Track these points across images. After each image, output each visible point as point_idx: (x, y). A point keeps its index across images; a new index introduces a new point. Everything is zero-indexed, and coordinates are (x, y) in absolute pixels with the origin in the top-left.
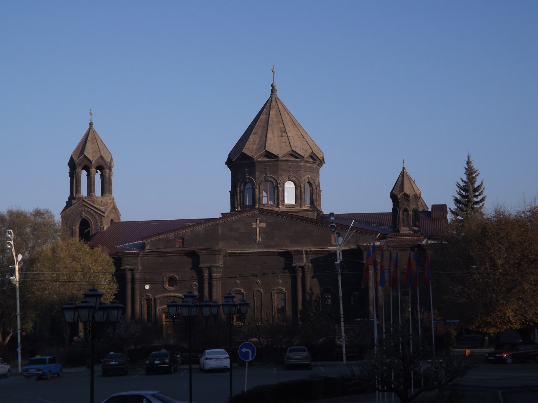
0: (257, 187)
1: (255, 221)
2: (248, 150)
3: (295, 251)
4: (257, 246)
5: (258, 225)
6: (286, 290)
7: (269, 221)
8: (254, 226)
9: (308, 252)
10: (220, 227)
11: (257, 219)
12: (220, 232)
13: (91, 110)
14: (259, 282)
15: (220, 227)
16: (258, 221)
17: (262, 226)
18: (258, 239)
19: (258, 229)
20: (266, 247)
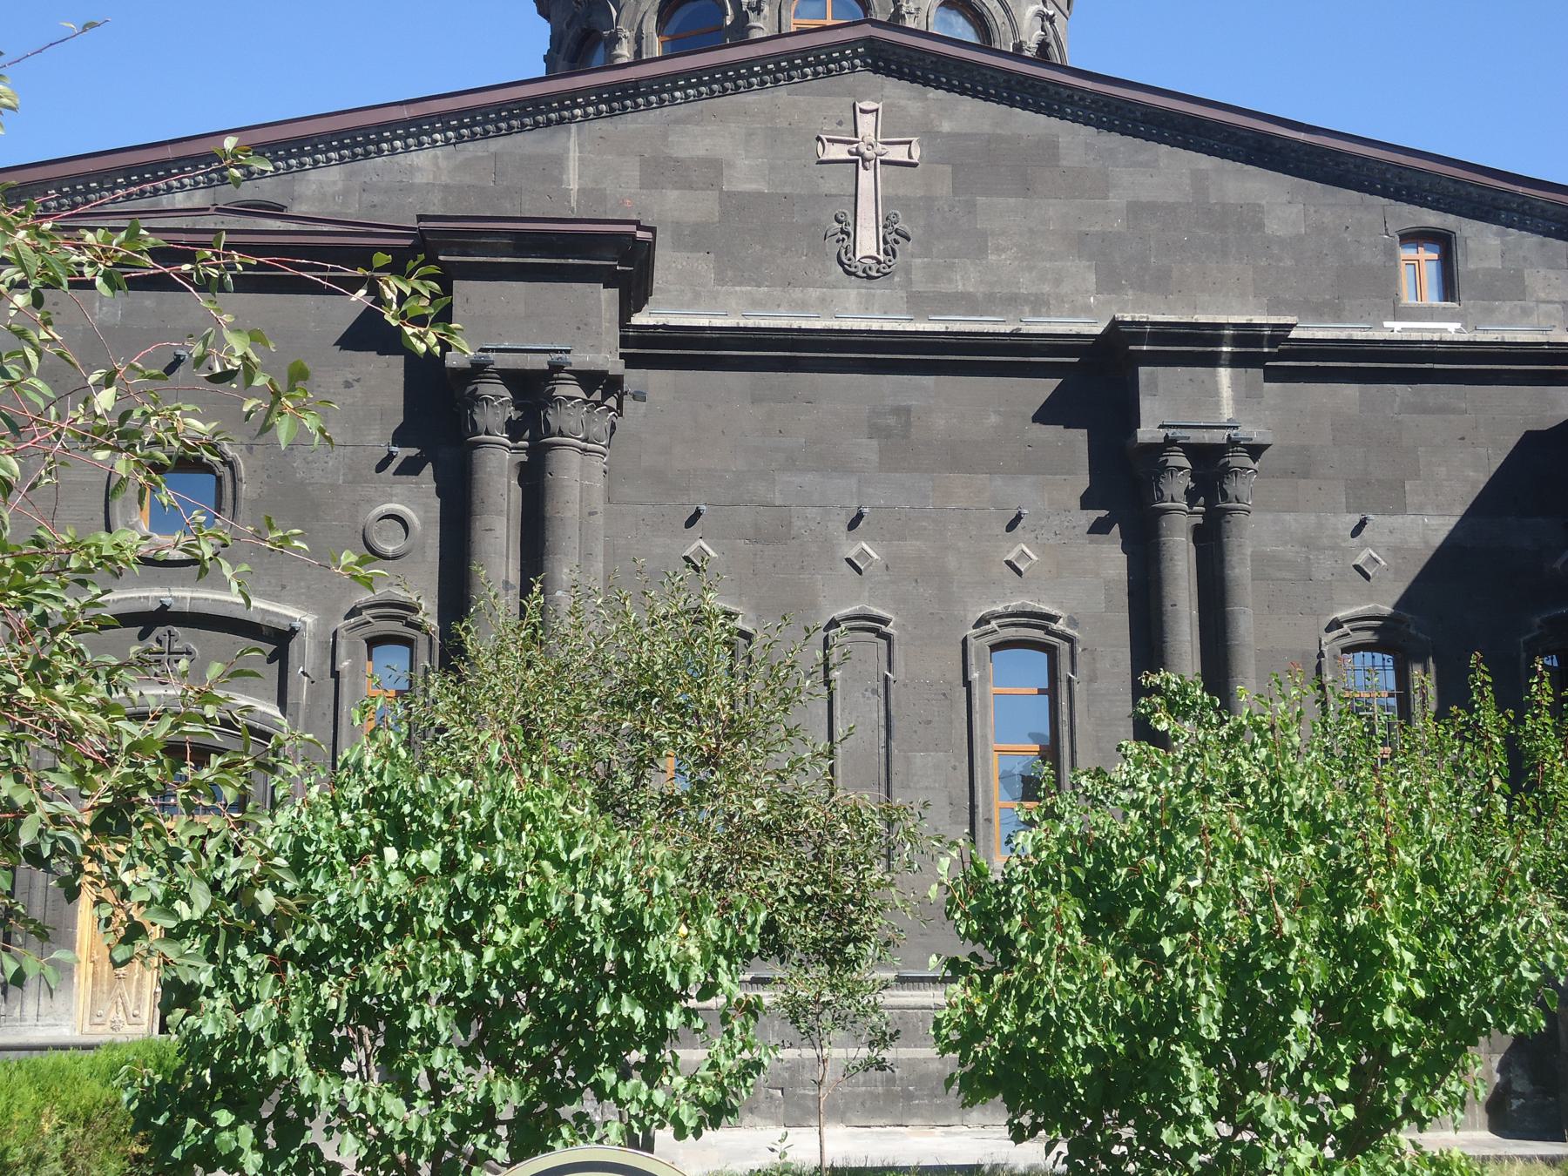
0: (766, 9)
1: (840, 123)
3: (1165, 333)
4: (853, 293)
6: (1072, 622)
7: (946, 127)
8: (839, 152)
10: (573, 144)
11: (859, 105)
12: (573, 181)
14: (863, 554)
15: (573, 144)
16: (866, 124)
17: (898, 153)
18: (867, 243)
19: (866, 177)
20: (918, 304)
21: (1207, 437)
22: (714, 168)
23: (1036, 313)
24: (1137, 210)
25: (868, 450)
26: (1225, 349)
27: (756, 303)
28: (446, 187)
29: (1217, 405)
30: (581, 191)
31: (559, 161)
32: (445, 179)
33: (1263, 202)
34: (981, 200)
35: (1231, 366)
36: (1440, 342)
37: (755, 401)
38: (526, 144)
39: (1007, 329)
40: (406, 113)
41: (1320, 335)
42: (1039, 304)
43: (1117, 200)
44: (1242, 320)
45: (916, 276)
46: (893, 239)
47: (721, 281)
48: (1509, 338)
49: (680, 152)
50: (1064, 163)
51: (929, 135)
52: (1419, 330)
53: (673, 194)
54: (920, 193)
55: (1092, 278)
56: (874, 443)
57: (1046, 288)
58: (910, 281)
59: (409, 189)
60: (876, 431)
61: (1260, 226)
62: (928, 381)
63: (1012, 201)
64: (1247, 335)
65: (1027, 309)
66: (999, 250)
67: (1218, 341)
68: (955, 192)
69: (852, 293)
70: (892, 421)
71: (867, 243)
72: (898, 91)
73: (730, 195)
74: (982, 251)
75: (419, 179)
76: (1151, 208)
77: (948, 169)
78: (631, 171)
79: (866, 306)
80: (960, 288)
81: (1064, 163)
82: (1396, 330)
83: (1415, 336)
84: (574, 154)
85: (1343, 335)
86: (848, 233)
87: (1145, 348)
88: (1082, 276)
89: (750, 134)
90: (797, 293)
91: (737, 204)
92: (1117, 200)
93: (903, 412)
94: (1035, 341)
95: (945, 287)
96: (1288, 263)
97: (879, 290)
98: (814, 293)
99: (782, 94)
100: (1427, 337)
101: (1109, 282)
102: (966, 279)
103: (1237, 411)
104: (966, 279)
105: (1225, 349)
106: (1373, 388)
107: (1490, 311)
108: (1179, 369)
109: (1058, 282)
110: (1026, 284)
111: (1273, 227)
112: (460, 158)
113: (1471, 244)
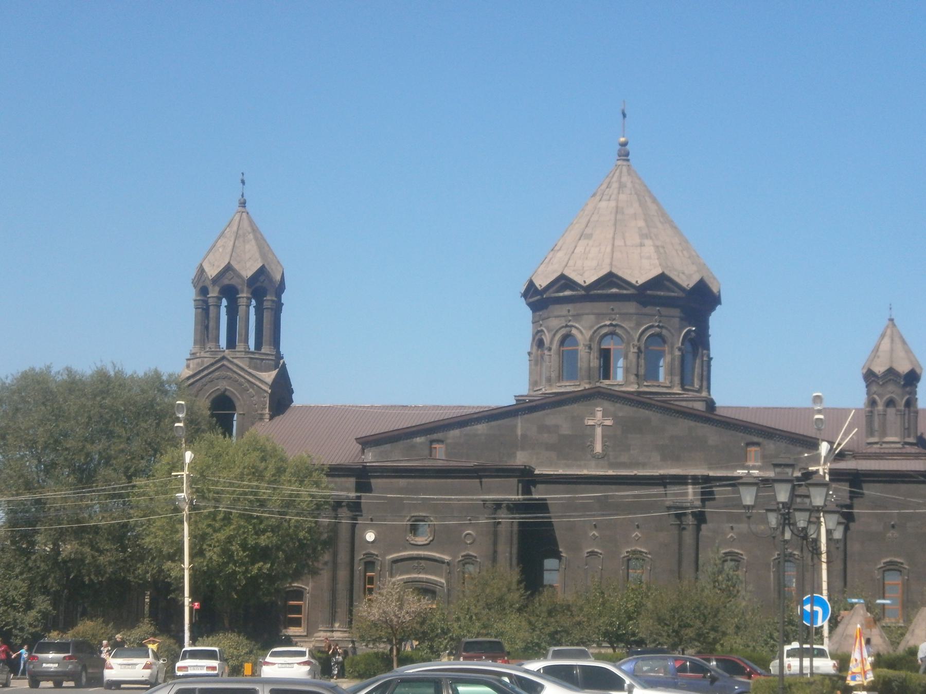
2: (574, 271)
5: (599, 423)
7: (620, 414)
8: (591, 423)
9: (699, 479)
12: (519, 432)
13: (243, 174)
18: (598, 448)
19: (599, 431)
20: (612, 466)
30: (521, 435)
31: (515, 426)
42: (644, 465)
51: (615, 418)
53: (546, 435)
67: (688, 479)
69: (593, 463)
71: (598, 448)
72: (607, 404)
75: (480, 432)
84: (519, 424)
99: (576, 405)
102: (624, 458)
104: (624, 458)
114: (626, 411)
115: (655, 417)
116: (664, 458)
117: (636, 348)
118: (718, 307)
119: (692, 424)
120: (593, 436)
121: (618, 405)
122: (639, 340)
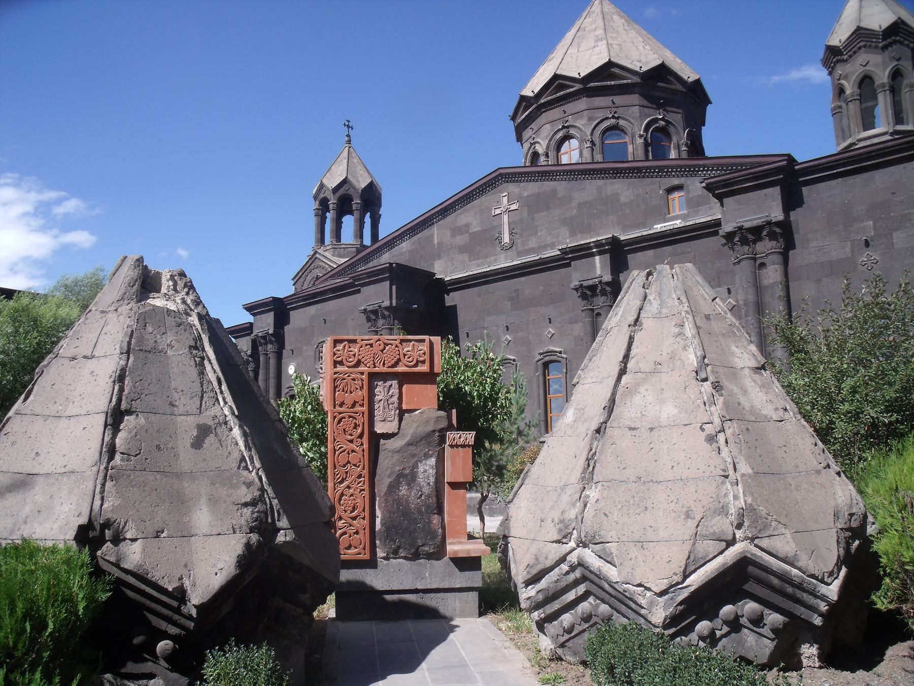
4: (502, 256)
7: (525, 194)
8: (498, 211)
10: (435, 230)
15: (435, 230)
18: (506, 239)
20: (520, 254)
21: (591, 283)
22: (467, 225)
23: (552, 249)
24: (580, 205)
25: (508, 305)
26: (594, 250)
27: (479, 265)
28: (409, 251)
29: (595, 270)
31: (432, 236)
32: (409, 249)
33: (619, 192)
34: (535, 215)
35: (599, 255)
36: (673, 229)
37: (480, 295)
38: (425, 233)
39: (537, 258)
40: (397, 234)
41: (632, 236)
43: (574, 204)
44: (594, 240)
45: (519, 245)
46: (511, 234)
47: (470, 261)
48: (697, 222)
49: (459, 225)
50: (558, 196)
52: (668, 226)
53: (458, 237)
54: (519, 218)
55: (568, 233)
56: (510, 303)
57: (555, 240)
58: (517, 248)
59: (401, 254)
60: (510, 299)
61: (619, 200)
62: (523, 279)
63: (544, 213)
64: (598, 244)
65: (549, 248)
66: (541, 230)
67: (591, 248)
68: (529, 214)
70: (514, 294)
71: (506, 239)
72: (512, 187)
73: (473, 233)
74: (536, 232)
76: (585, 203)
77: (527, 208)
78: (449, 234)
79: (506, 259)
80: (531, 246)
81: (558, 196)
82: (659, 227)
83: (664, 229)
84: (436, 233)
85: (640, 235)
86: (499, 239)
87: (570, 256)
88: (565, 232)
89: (476, 213)
90: (488, 260)
91: (473, 236)
92: (574, 204)
93: (517, 291)
94: (547, 260)
95: (527, 247)
96: (628, 211)
97: (510, 253)
98: (493, 258)
99: (483, 198)
100: (668, 228)
101: (573, 234)
102: (532, 244)
103: (602, 271)
105: (594, 250)
106: (658, 250)
107: (698, 211)
108: (583, 260)
109: (558, 237)
110: (549, 240)
111: (623, 200)
112: (412, 241)
113: (690, 187)
114: (531, 188)
115: (560, 187)
116: (573, 234)
117: (589, 142)
118: (709, 108)
119: (600, 182)
120: (501, 225)
121: (522, 184)
122: (592, 134)
